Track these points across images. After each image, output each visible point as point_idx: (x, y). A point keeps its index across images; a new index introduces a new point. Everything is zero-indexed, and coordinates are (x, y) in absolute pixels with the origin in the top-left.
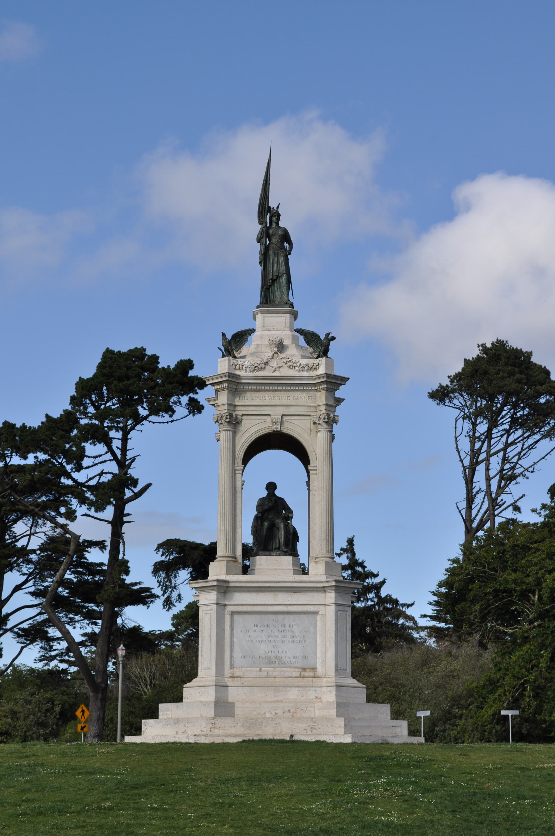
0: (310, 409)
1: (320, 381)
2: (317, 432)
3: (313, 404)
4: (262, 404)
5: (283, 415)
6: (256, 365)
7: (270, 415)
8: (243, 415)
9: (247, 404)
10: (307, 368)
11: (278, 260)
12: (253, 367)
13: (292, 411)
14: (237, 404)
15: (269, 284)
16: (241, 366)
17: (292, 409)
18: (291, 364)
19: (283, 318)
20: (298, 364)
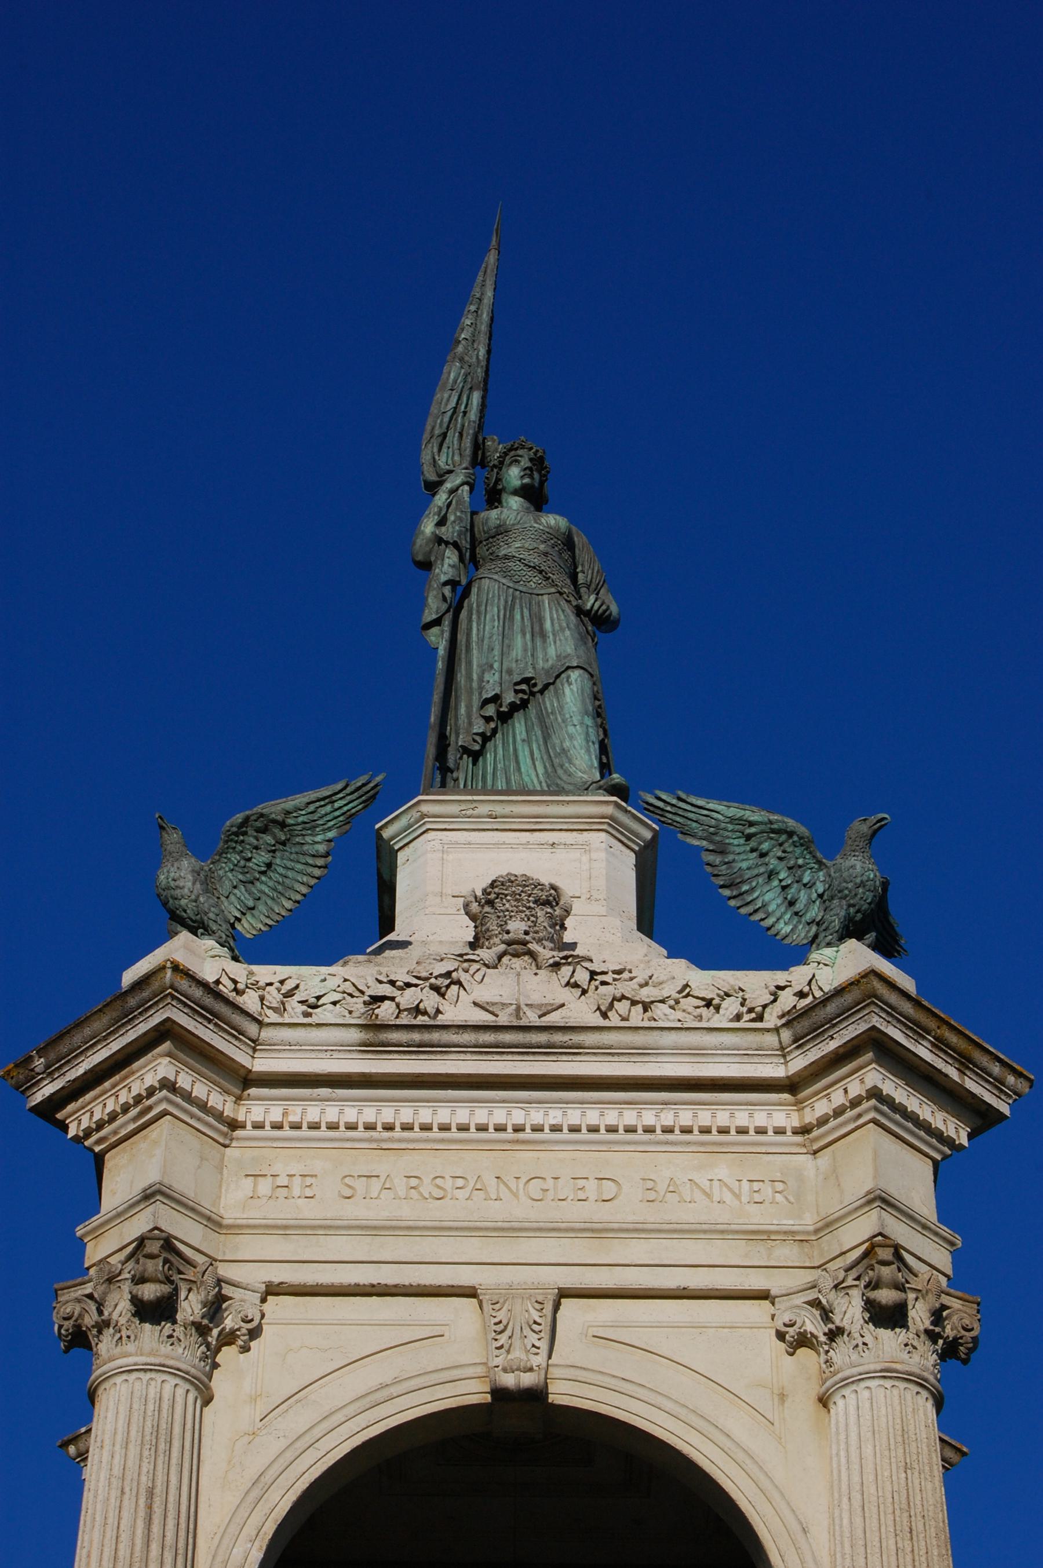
0: (758, 1254)
1: (833, 1045)
2: (824, 1401)
3: (788, 1223)
4: (406, 1212)
5: (564, 1294)
6: (386, 990)
7: (470, 1293)
8: (272, 1290)
9: (309, 1211)
10: (731, 1007)
11: (537, 619)
12: (358, 1004)
13: (633, 1261)
14: (229, 1214)
15: (479, 726)
16: (273, 996)
17: (638, 1250)
18: (624, 988)
19: (561, 854)
20: (670, 990)
